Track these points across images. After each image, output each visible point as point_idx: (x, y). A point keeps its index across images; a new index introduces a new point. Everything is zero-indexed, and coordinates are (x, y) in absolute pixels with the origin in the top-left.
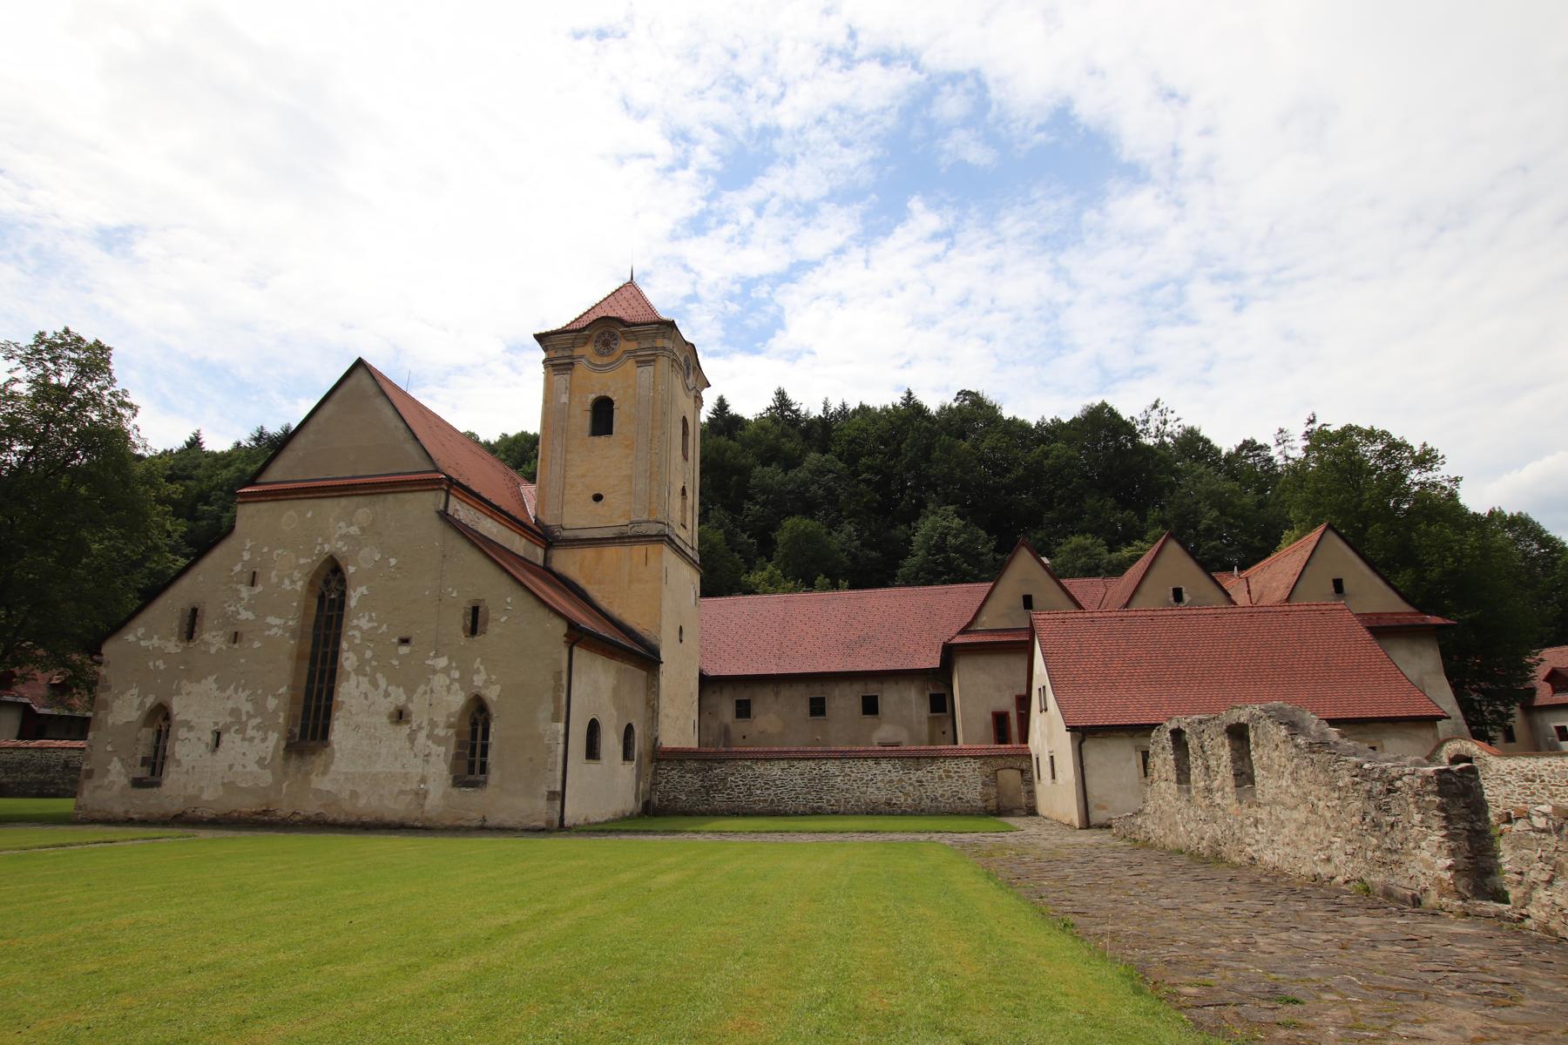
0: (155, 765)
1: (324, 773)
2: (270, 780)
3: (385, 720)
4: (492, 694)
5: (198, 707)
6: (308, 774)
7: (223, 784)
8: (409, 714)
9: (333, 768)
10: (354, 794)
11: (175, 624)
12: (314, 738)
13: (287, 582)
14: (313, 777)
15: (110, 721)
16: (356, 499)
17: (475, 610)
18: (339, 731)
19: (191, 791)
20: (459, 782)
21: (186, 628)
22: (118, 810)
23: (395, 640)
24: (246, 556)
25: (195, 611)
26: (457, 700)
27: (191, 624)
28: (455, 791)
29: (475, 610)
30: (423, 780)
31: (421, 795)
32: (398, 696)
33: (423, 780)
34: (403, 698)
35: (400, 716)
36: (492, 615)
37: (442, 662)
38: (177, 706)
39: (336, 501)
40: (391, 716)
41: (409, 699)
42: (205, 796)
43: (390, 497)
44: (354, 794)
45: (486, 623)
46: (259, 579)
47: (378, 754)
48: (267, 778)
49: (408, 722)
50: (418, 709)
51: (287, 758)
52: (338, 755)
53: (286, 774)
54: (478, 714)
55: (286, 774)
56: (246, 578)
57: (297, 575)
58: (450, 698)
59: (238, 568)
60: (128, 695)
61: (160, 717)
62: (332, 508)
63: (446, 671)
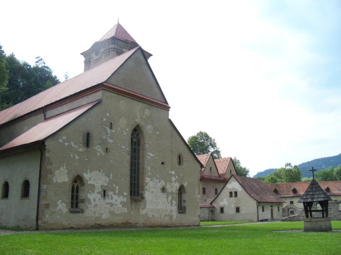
0: (76, 202)
1: (143, 209)
2: (127, 211)
3: (160, 191)
4: (185, 185)
5: (95, 179)
6: (139, 209)
7: (110, 212)
8: (166, 189)
9: (147, 207)
10: (153, 216)
11: (81, 138)
12: (135, 195)
13: (124, 132)
14: (140, 210)
15: (55, 181)
16: (144, 105)
17: (180, 156)
18: (147, 195)
19: (97, 215)
20: (179, 213)
21: (86, 141)
22: (65, 223)
23: (160, 162)
24: (108, 115)
25: (88, 134)
26: (177, 185)
27: (88, 140)
28: (179, 215)
29: (180, 156)
30: (171, 211)
31: (171, 217)
32: (163, 183)
33: (171, 211)
34: (164, 184)
35: (163, 190)
36: (184, 159)
37: (173, 172)
38: (86, 176)
39: (138, 103)
40: (161, 190)
41: (166, 184)
42: (104, 216)
43: (155, 108)
44: (153, 216)
45: (183, 162)
46: (113, 127)
47: (159, 202)
48: (125, 210)
49: (166, 192)
50: (169, 189)
51: (131, 203)
52: (147, 202)
53: (132, 208)
54: (181, 190)
55: (132, 208)
56: (109, 124)
57: (127, 130)
58: (176, 185)
59: (105, 119)
60: (62, 169)
61: (78, 182)
62: (138, 106)
63: (174, 176)
